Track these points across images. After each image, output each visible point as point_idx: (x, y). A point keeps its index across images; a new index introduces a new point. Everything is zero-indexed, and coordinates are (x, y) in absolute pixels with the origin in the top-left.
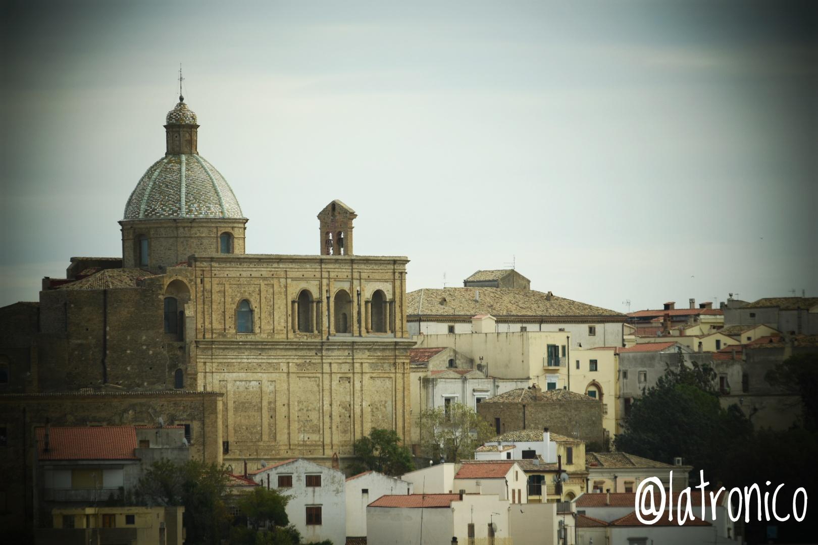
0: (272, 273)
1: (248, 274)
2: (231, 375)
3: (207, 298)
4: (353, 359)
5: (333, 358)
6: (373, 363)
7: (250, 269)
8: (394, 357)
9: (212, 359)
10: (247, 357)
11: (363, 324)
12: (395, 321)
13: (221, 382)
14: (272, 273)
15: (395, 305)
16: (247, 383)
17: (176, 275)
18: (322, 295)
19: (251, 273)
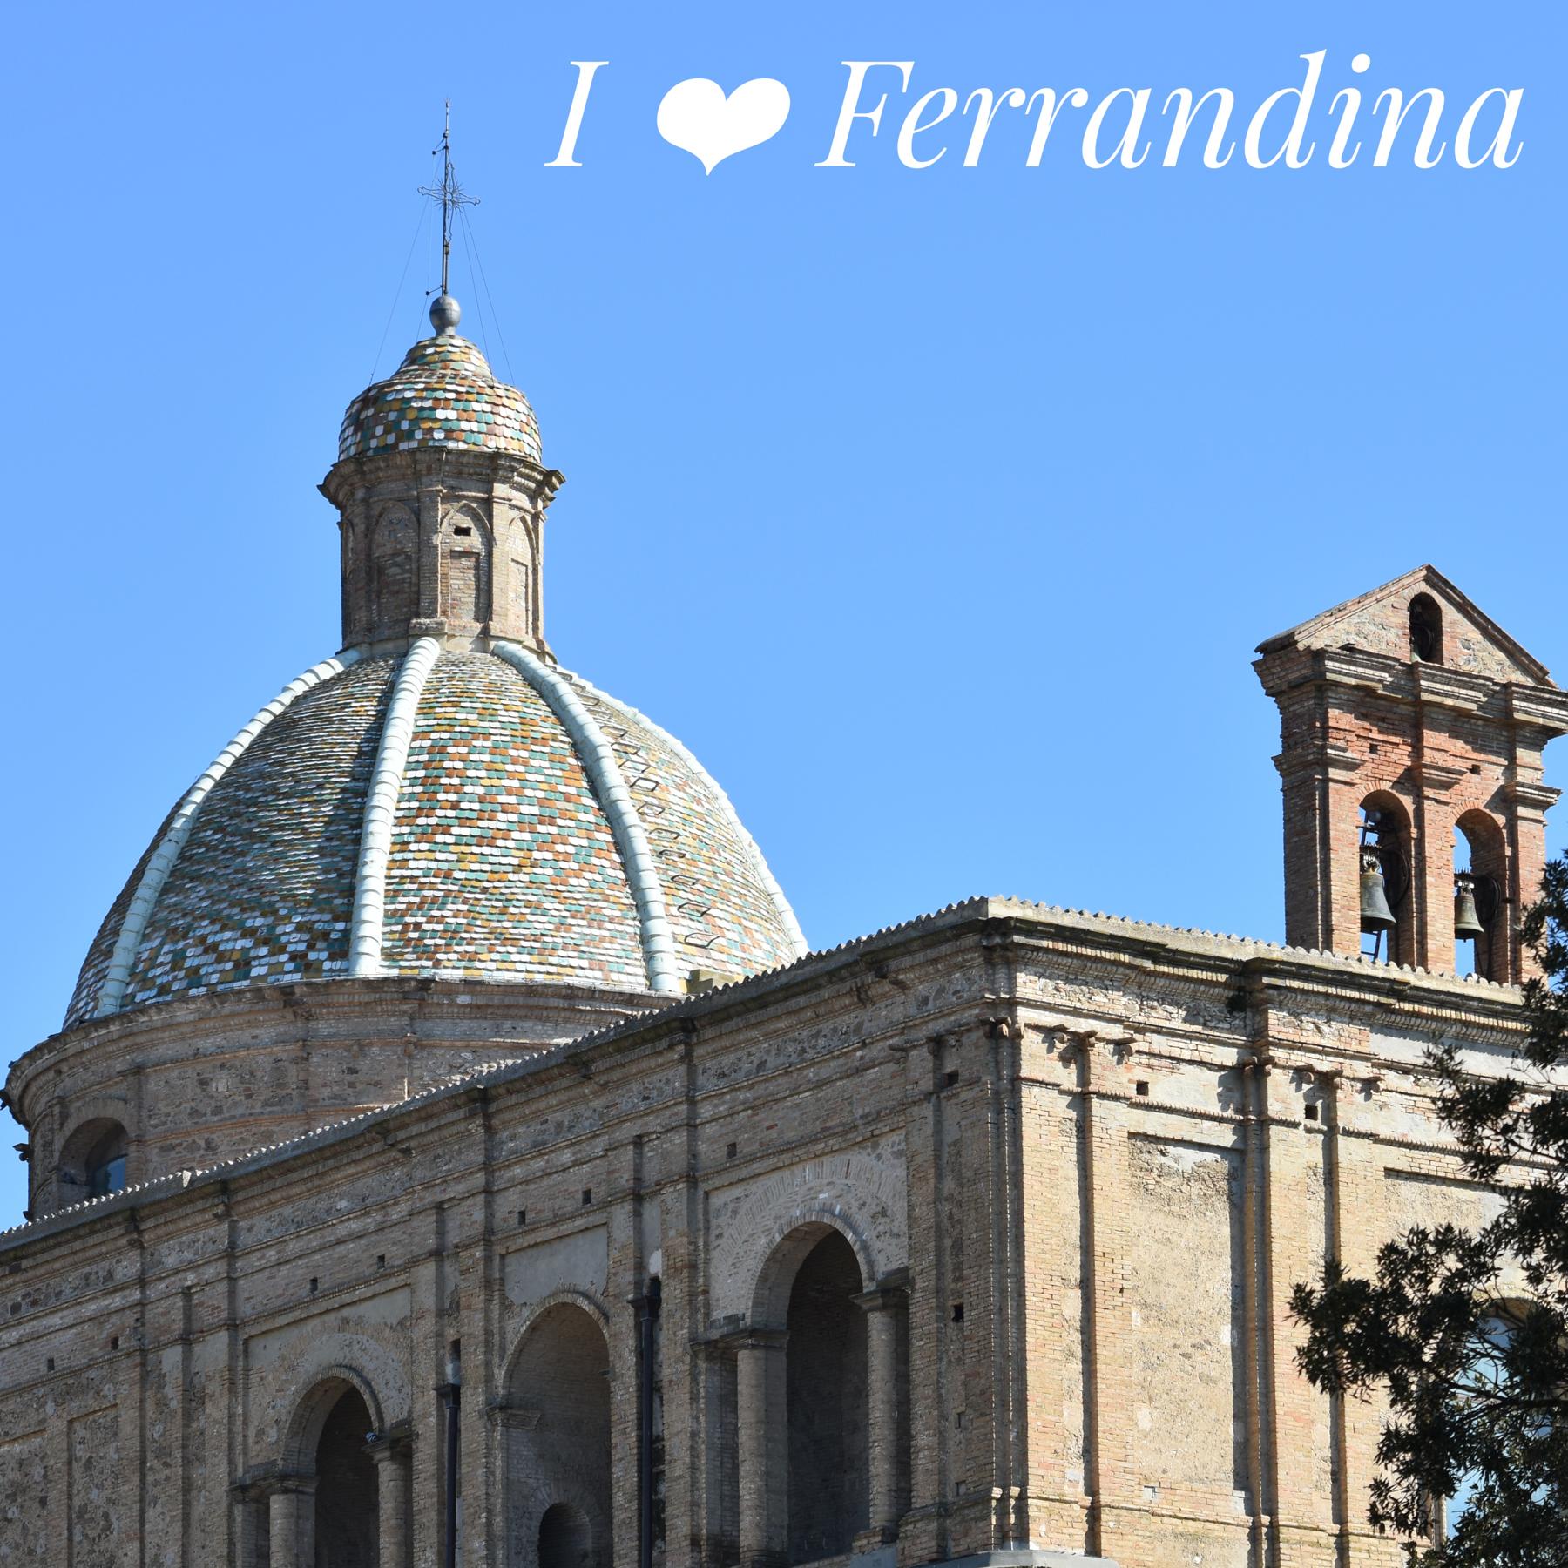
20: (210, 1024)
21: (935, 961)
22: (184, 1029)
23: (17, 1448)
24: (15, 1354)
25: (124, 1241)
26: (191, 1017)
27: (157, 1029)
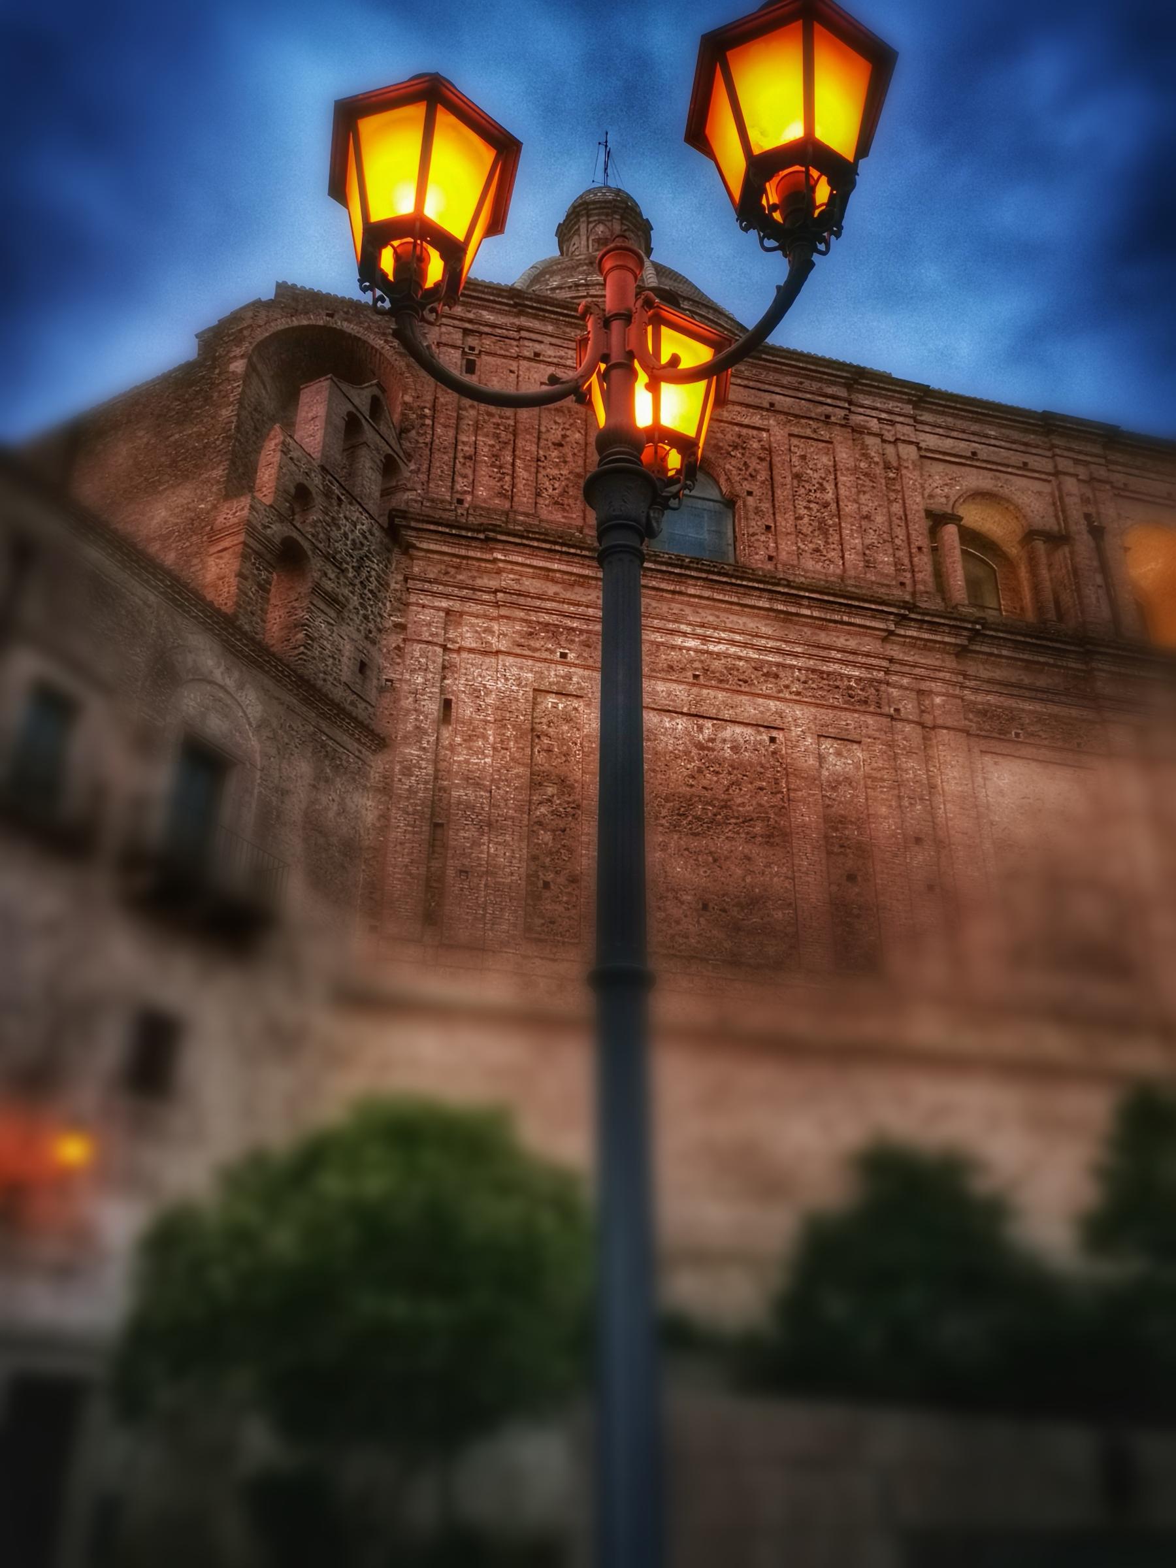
0: (821, 409)
10: (699, 631)
13: (551, 700)
16: (700, 729)
17: (331, 316)
23: (737, 429)
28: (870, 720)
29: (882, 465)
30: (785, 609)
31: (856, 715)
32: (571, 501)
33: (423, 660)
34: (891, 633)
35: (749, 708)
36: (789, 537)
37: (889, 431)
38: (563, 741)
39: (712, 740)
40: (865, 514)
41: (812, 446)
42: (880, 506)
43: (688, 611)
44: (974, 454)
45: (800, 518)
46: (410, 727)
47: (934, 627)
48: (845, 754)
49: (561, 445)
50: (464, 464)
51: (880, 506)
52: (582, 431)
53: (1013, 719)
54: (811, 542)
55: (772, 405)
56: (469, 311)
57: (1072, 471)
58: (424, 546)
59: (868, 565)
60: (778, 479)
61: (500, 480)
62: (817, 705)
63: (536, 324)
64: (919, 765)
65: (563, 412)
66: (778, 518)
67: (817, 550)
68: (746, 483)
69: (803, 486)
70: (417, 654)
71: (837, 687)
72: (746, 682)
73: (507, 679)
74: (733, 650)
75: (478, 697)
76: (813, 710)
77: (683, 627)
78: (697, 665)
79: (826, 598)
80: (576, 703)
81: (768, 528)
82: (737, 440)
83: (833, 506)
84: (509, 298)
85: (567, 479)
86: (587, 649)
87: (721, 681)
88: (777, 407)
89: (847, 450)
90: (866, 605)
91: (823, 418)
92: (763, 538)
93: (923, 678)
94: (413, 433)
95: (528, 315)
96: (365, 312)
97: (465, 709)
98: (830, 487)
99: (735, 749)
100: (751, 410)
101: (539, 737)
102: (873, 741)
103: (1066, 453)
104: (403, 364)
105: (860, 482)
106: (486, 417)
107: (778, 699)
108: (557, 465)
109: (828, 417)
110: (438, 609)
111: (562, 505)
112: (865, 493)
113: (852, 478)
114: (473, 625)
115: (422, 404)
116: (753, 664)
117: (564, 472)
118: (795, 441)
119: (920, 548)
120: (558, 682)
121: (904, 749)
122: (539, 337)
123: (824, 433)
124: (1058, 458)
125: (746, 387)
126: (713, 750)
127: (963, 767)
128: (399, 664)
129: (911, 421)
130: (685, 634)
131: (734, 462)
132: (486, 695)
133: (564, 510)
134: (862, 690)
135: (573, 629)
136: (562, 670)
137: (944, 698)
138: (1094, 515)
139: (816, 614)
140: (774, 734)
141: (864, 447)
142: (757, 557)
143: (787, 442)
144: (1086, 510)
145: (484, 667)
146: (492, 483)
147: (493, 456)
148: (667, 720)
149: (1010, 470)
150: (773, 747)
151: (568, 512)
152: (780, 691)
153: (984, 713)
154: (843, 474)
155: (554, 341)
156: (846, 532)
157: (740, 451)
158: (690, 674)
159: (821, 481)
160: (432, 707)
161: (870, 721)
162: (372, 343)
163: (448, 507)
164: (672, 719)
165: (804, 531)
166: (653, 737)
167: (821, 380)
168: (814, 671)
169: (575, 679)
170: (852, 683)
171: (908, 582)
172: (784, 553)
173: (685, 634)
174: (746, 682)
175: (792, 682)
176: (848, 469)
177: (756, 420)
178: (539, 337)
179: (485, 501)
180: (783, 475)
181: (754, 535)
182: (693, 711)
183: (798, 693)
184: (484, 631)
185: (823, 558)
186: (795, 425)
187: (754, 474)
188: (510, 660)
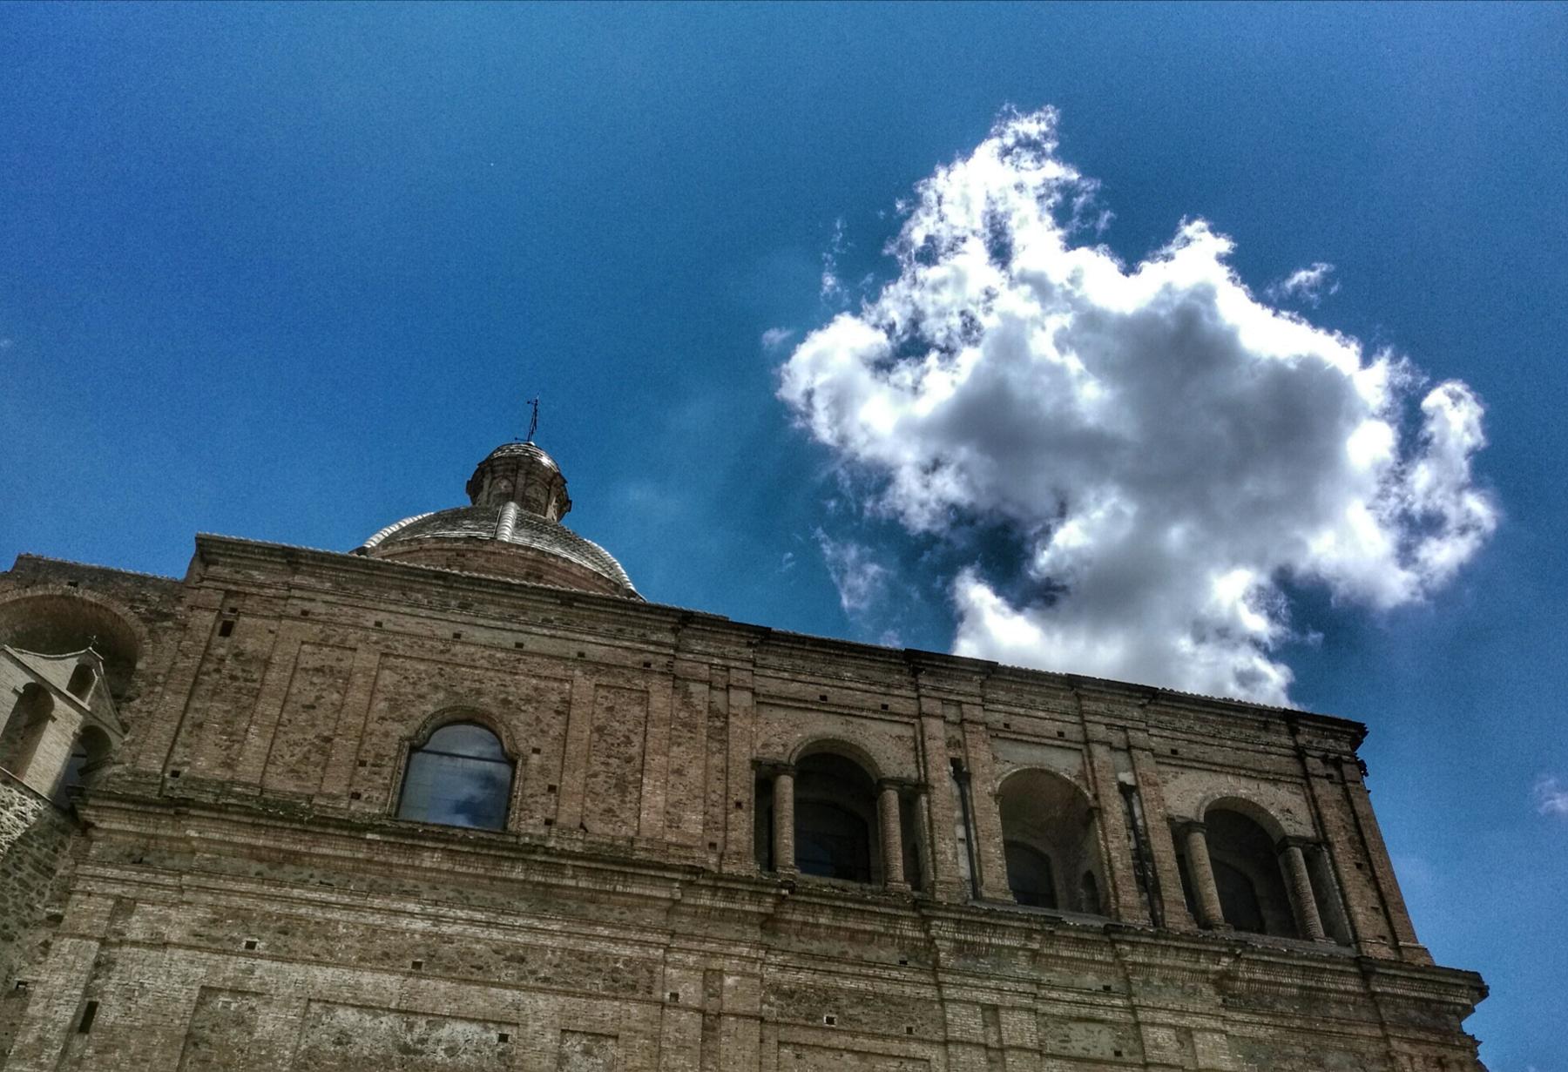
0: (641, 657)
1: (509, 639)
2: (296, 972)
3: (234, 678)
4: (1133, 1009)
5: (1007, 986)
6: (1260, 1041)
7: (516, 627)
8: (1378, 1032)
9: (181, 890)
11: (1173, 891)
12: (1347, 907)
14: (641, 657)
15: (1332, 857)
16: (410, 1027)
18: (925, 768)
19: (522, 638)
20: (585, 583)
21: (1326, 729)
22: (571, 578)
23: (534, 681)
24: (546, 640)
25: (669, 626)
26: (579, 574)
27: (556, 567)
28: (634, 1009)
29: (706, 712)
30: (543, 880)
31: (617, 1003)
32: (310, 769)
33: (71, 958)
34: (676, 902)
35: (478, 999)
36: (574, 797)
37: (722, 677)
38: (225, 1048)
39: (423, 1041)
40: (676, 767)
41: (623, 696)
42: (696, 758)
43: (423, 887)
44: (824, 698)
45: (595, 775)
46: (30, 1039)
47: (730, 894)
48: (596, 1051)
49: (314, 707)
50: (191, 732)
51: (696, 758)
52: (342, 692)
53: (826, 1000)
54: (603, 802)
55: (581, 655)
56: (237, 572)
57: (939, 712)
58: (105, 825)
59: (673, 823)
60: (573, 733)
61: (228, 748)
62: (567, 993)
63: (313, 581)
64: (692, 1061)
65: (323, 672)
66: (565, 777)
67: (610, 810)
68: (533, 739)
69: (605, 741)
70: (65, 950)
71: (599, 970)
72: (480, 968)
73: (169, 975)
74: (471, 930)
75: (130, 999)
76: (561, 999)
77: (411, 907)
78: (421, 950)
79: (593, 865)
80: (254, 1002)
81: (552, 789)
82: (534, 694)
83: (638, 761)
84: (282, 557)
85: (313, 743)
86: (282, 937)
87: (448, 969)
88: (589, 656)
89: (664, 699)
90: (645, 872)
91: (641, 666)
92: (543, 799)
93: (714, 954)
94: (138, 701)
95: (303, 573)
96: (115, 580)
97: (109, 1014)
98: (637, 740)
99: (452, 1051)
100: (554, 661)
101: (196, 1044)
102: (633, 1034)
103: (934, 694)
104: (145, 630)
105: (674, 733)
106: (228, 682)
107: (517, 987)
108: (303, 730)
109: (647, 665)
110: (107, 896)
111: (298, 772)
112: (679, 745)
113: (665, 730)
114: (146, 914)
115: (156, 671)
116: (494, 947)
117: (310, 736)
118: (602, 692)
119: (739, 805)
120: (235, 977)
121: (675, 1043)
122: (311, 595)
123: (640, 683)
124: (923, 699)
125: (552, 637)
126: (421, 1053)
127: (750, 1063)
128: (40, 963)
129: (749, 666)
130: (412, 914)
131: (522, 716)
132: (141, 996)
133: (300, 778)
134: (631, 972)
135: (270, 914)
136: (243, 963)
137: (738, 978)
138: (964, 760)
139: (582, 884)
140: (506, 1030)
141: (688, 694)
142: (531, 821)
143: (592, 693)
144: (952, 754)
145: (146, 963)
146: (216, 751)
147: (227, 722)
148: (368, 1018)
149: (864, 714)
150: (502, 1046)
151: (303, 780)
152: (522, 978)
153: (791, 994)
154: (654, 726)
155: (329, 598)
156: (646, 789)
157: (534, 705)
158: (409, 962)
159: (627, 733)
160: (66, 1014)
161: (634, 1010)
162: (115, 610)
163: (154, 781)
164: (376, 1016)
165: (598, 789)
166: (345, 1040)
167: (644, 627)
168: (571, 952)
169: (257, 973)
170: (619, 965)
171: (719, 842)
172: (565, 815)
173: (412, 914)
174: (480, 968)
175: (541, 966)
176: (661, 719)
177: (560, 671)
178: (311, 595)
179: (203, 772)
180: (582, 731)
181: (532, 796)
182: (404, 1006)
183: (546, 980)
184: (158, 921)
185: (614, 819)
186: (606, 674)
187: (546, 728)
188: (181, 952)
